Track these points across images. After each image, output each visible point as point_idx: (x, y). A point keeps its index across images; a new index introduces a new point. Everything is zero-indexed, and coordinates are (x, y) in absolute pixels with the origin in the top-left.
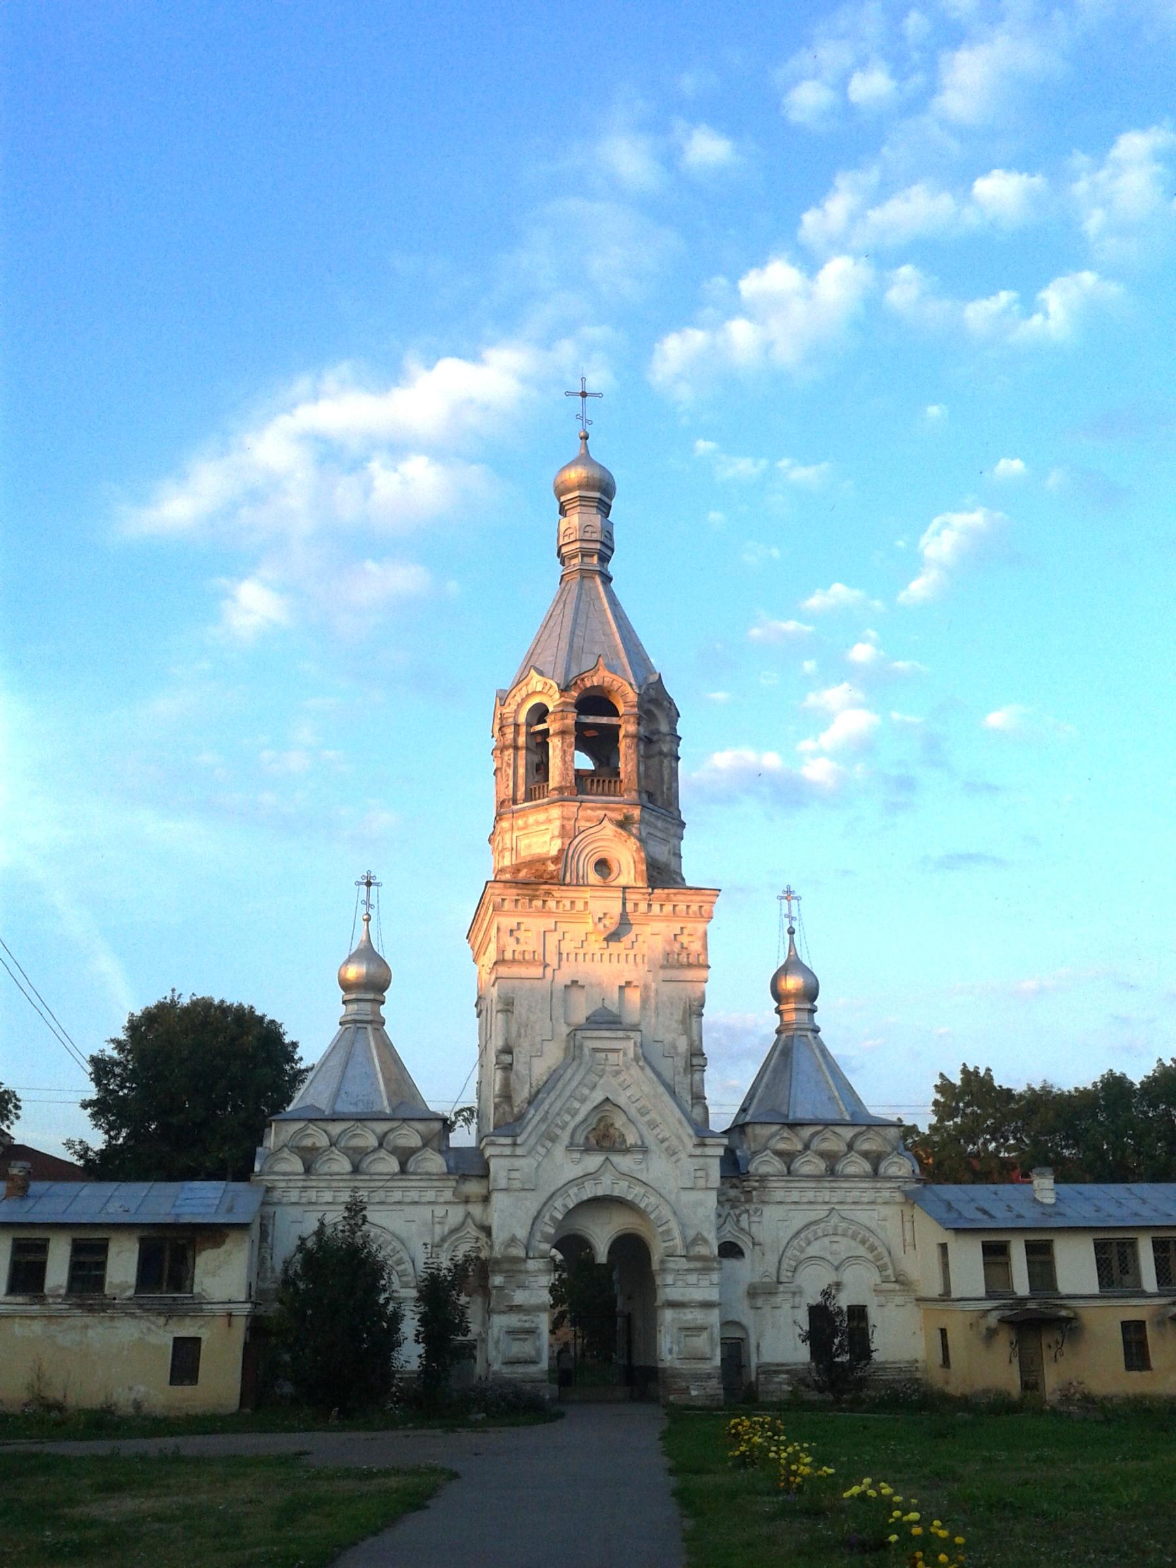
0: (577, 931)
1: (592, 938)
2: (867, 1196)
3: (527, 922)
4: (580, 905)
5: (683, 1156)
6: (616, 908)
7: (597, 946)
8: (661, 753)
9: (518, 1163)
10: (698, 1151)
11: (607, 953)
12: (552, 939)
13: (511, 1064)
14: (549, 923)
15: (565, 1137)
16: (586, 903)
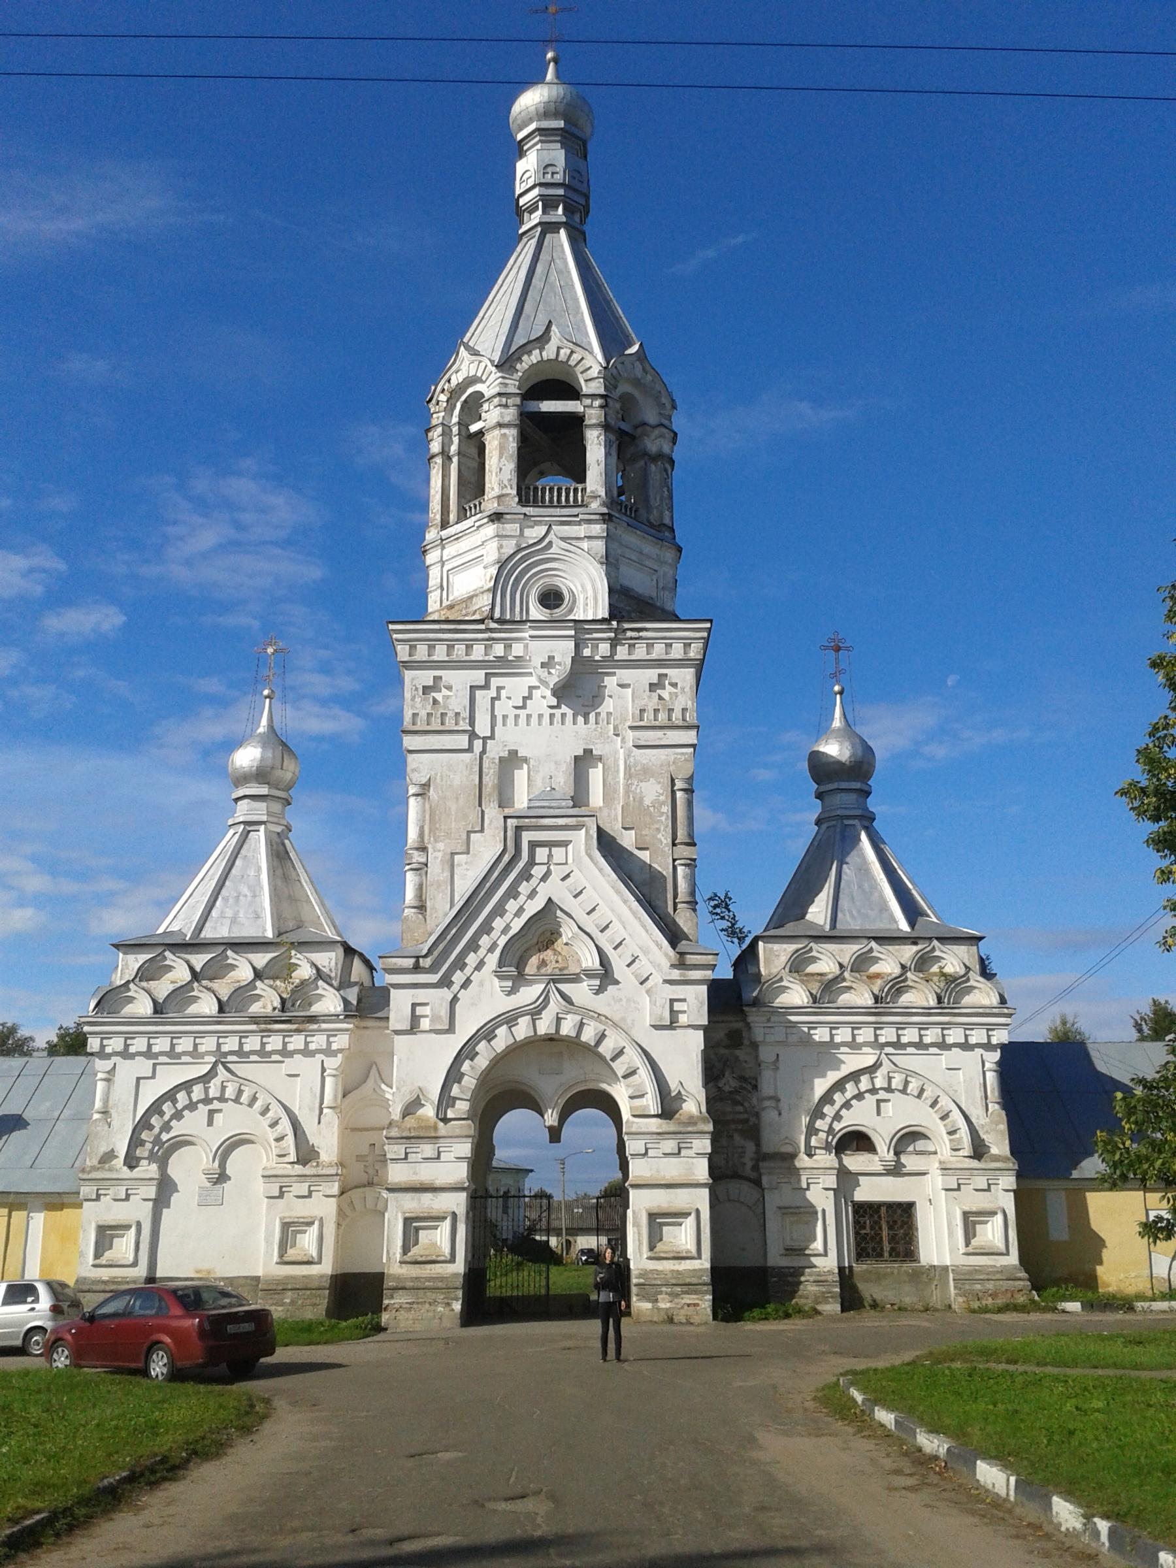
0: (515, 687)
1: (537, 694)
2: (931, 1036)
3: (448, 676)
4: (517, 650)
5: (657, 979)
6: (564, 650)
7: (545, 703)
8: (645, 454)
9: (422, 995)
10: (676, 974)
11: (558, 712)
12: (483, 697)
13: (426, 865)
14: (478, 676)
15: (492, 960)
16: (526, 647)
